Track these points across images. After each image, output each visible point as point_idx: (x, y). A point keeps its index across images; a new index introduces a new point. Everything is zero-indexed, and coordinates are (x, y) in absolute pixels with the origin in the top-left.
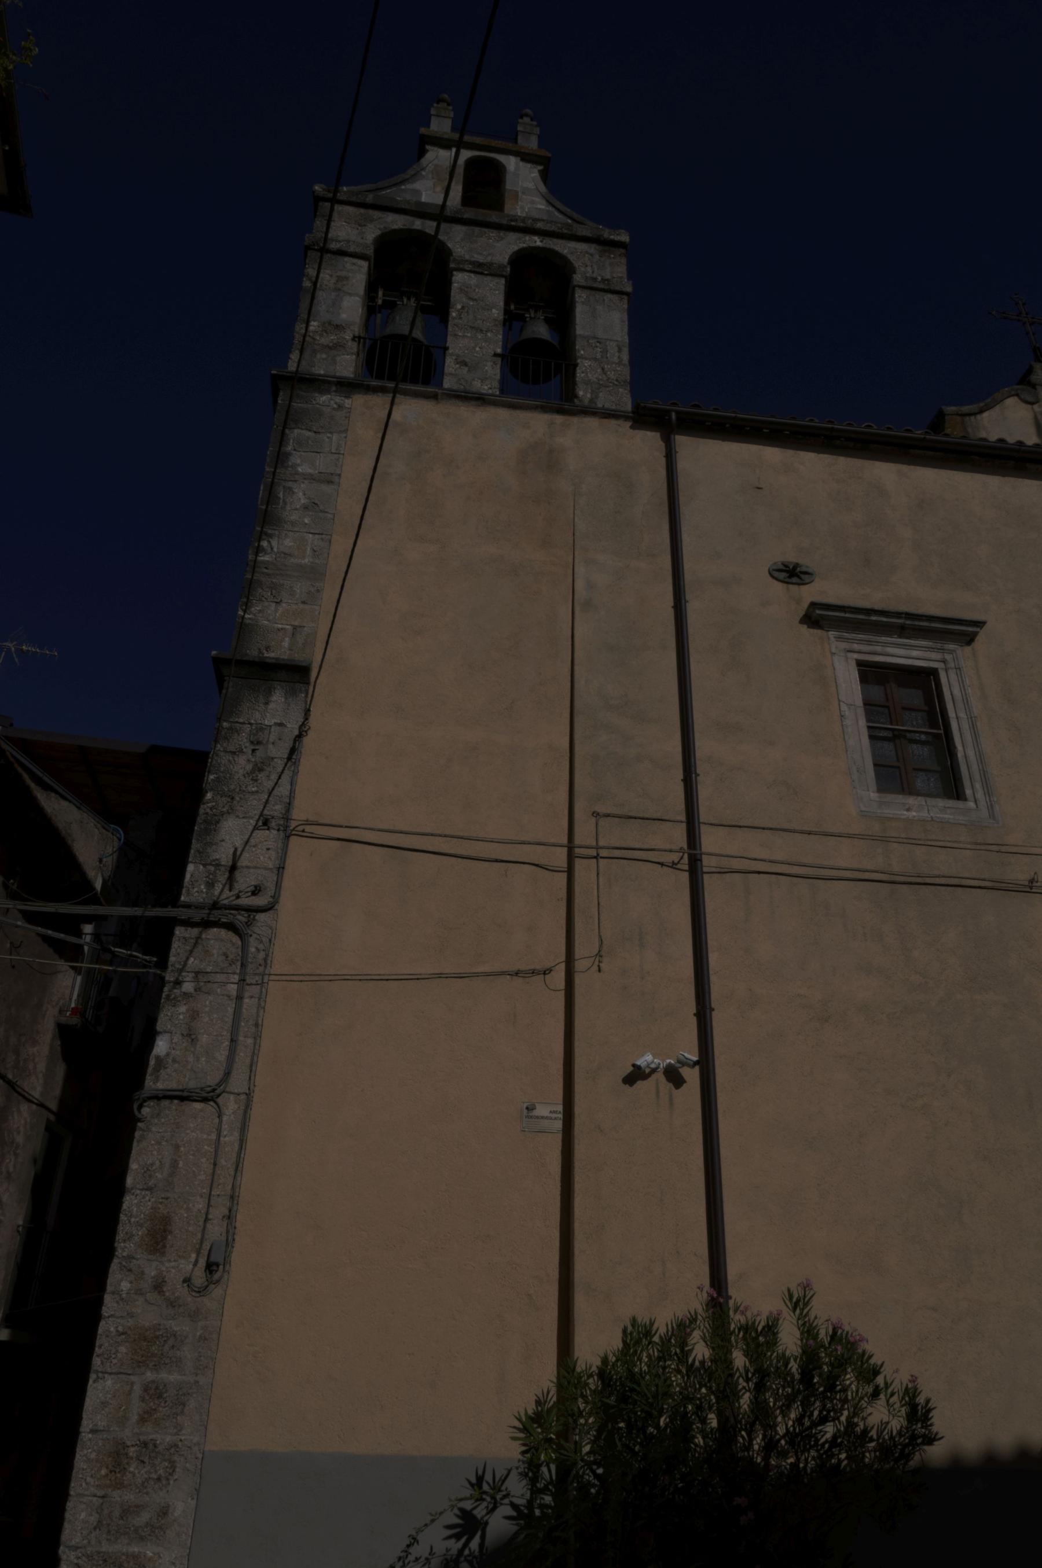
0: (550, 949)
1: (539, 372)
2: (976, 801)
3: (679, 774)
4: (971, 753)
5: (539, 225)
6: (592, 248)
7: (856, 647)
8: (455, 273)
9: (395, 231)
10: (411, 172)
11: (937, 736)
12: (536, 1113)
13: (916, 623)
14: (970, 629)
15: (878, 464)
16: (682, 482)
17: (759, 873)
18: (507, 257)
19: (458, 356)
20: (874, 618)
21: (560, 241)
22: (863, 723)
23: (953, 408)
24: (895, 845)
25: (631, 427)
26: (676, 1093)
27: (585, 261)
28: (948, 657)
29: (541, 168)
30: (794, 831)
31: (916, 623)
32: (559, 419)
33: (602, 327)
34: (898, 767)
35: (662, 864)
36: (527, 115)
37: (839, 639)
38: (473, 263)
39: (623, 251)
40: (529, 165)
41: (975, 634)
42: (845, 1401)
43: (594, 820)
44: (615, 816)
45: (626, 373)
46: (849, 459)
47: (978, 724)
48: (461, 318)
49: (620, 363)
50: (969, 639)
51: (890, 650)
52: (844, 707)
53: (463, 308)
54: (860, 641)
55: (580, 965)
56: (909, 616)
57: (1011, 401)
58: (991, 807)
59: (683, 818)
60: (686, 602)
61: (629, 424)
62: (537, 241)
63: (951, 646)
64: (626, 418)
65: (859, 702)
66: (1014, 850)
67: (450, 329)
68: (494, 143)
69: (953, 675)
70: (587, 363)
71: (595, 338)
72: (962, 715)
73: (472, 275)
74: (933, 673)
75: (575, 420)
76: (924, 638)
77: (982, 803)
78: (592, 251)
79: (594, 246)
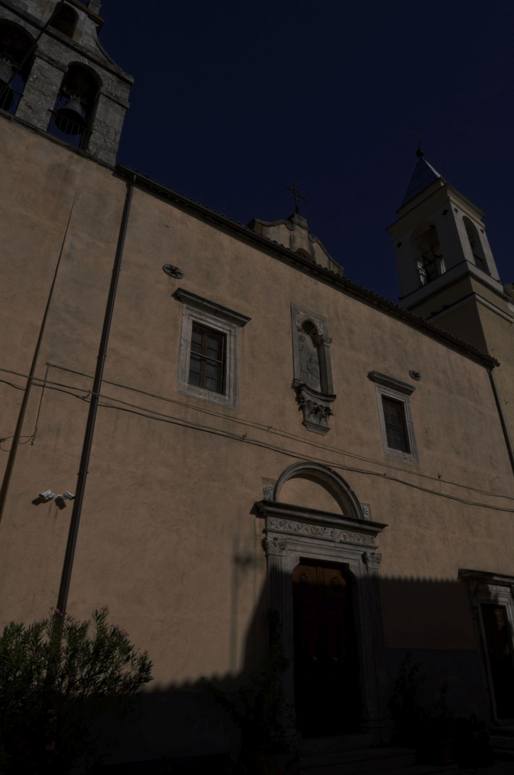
1: (71, 127)
2: (229, 397)
3: (97, 354)
4: (232, 375)
5: (89, 54)
6: (114, 78)
7: (194, 314)
8: (37, 58)
9: (7, 20)
11: (219, 364)
13: (223, 311)
14: (244, 320)
15: (223, 234)
16: (132, 211)
17: (125, 410)
18: (68, 63)
20: (205, 303)
21: (98, 67)
22: (189, 350)
24: (191, 409)
25: (112, 174)
26: (59, 511)
27: (108, 82)
28: (232, 330)
29: (98, 25)
30: (147, 394)
31: (223, 311)
32: (76, 156)
33: (109, 120)
34: (200, 374)
35: (78, 396)
37: (187, 308)
38: (49, 57)
39: (129, 86)
40: (91, 21)
41: (246, 322)
42: (112, 663)
43: (46, 367)
44: (58, 367)
45: (116, 147)
47: (238, 363)
48: (34, 83)
49: (114, 141)
50: (242, 324)
51: (208, 320)
52: (182, 341)
53: (37, 78)
55: (22, 440)
56: (220, 306)
57: (283, 226)
61: (112, 172)
62: (86, 62)
63: (235, 325)
64: (111, 169)
65: (190, 340)
67: (27, 86)
69: (232, 338)
70: (97, 134)
71: (104, 123)
72: (232, 357)
73: (47, 63)
74: (225, 335)
75: (85, 160)
76: (225, 318)
78: (114, 79)
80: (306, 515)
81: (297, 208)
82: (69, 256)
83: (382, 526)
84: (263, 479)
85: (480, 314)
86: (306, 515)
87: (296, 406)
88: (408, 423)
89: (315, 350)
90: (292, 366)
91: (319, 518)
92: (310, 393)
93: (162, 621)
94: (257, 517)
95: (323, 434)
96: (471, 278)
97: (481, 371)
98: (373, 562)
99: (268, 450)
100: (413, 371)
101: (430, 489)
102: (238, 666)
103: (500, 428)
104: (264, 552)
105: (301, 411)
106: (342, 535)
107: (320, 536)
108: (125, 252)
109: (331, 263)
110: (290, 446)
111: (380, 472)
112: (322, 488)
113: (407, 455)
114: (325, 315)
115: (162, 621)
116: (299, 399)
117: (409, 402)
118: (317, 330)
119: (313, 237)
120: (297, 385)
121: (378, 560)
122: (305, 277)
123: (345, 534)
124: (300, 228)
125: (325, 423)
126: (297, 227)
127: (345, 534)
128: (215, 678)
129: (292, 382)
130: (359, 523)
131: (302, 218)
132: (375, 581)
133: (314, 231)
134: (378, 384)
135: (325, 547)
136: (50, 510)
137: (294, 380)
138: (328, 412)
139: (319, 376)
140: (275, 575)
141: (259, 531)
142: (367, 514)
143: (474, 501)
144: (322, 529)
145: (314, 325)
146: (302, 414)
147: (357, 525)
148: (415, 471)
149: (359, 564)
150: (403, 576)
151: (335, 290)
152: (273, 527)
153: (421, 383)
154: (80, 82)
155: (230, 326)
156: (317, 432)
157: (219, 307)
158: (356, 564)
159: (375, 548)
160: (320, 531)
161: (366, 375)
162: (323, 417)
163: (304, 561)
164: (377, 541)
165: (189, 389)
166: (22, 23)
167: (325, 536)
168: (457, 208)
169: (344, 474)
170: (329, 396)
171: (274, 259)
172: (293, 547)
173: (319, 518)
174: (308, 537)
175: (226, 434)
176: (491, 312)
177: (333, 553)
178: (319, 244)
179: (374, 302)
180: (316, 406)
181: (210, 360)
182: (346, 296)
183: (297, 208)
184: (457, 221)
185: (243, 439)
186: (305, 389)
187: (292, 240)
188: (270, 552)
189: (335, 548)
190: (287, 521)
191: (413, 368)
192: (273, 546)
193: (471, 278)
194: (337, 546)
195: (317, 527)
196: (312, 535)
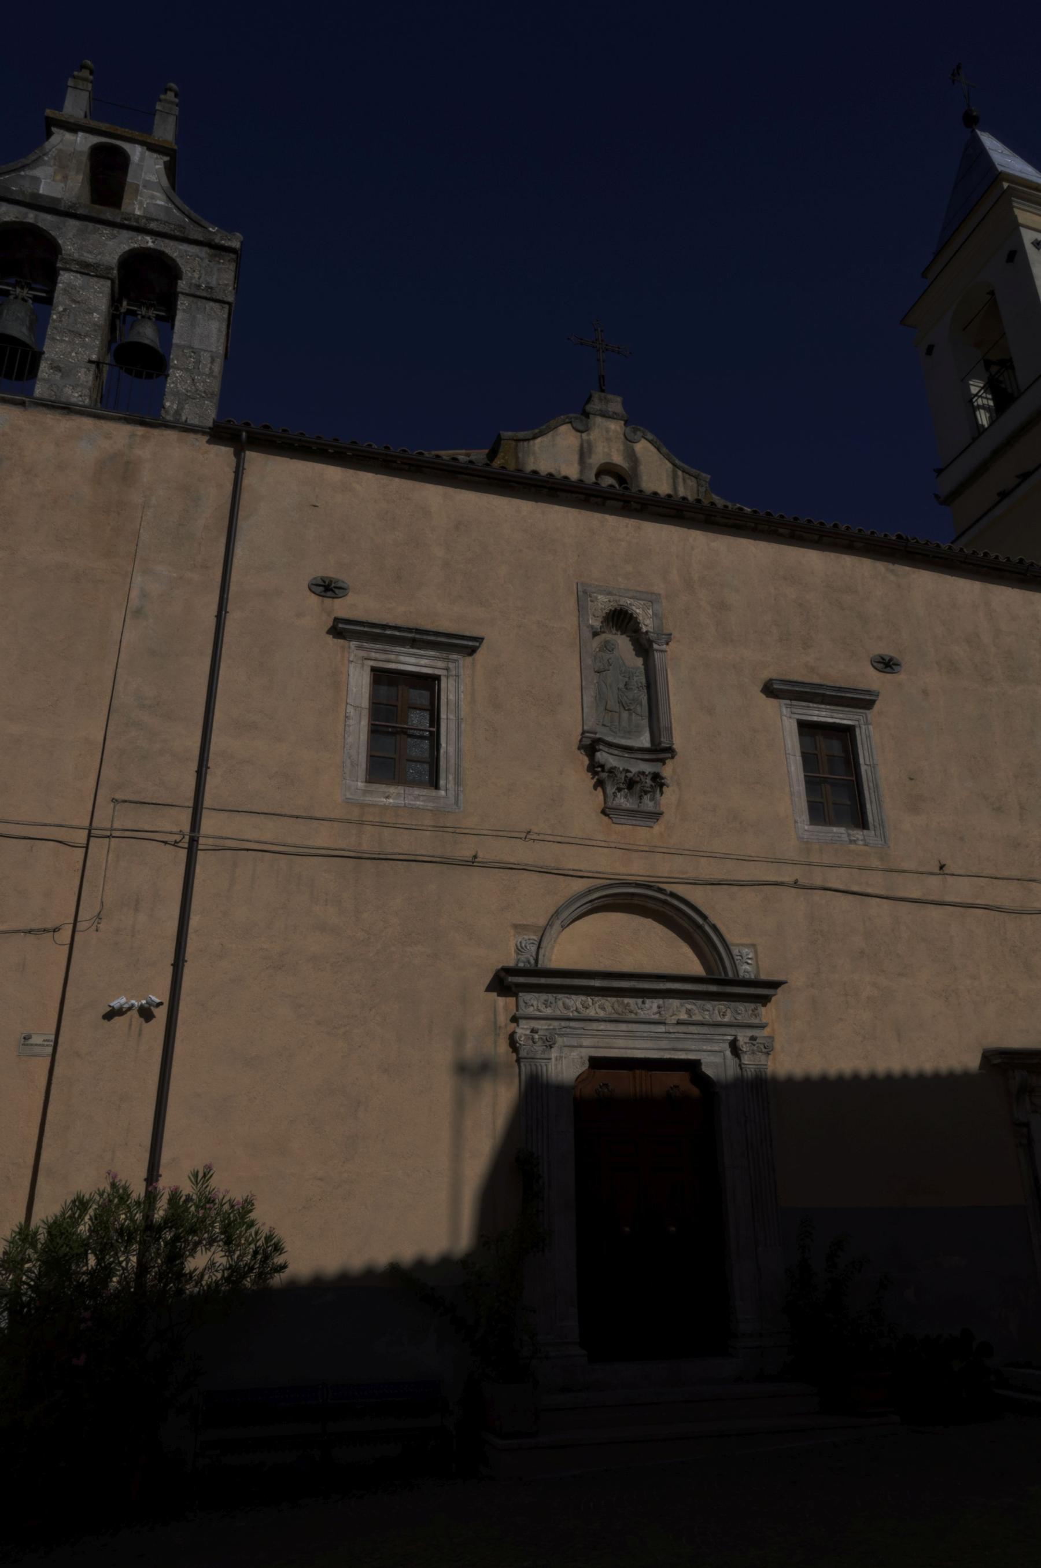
0: (62, 912)
1: (133, 379)
3: (194, 766)
4: (452, 750)
5: (153, 226)
6: (204, 252)
7: (373, 655)
8: (61, 272)
9: (7, 223)
10: (32, 157)
12: (30, 1042)
14: (470, 643)
16: (245, 498)
17: (248, 850)
18: (117, 257)
19: (53, 360)
20: (388, 632)
21: (172, 243)
22: (365, 723)
23: (509, 434)
24: (369, 827)
25: (208, 442)
26: (145, 1025)
27: (195, 267)
28: (451, 665)
29: (166, 159)
30: (285, 816)
32: (140, 430)
33: (199, 336)
35: (165, 843)
36: (171, 90)
37: (359, 648)
39: (234, 256)
40: (155, 155)
42: (239, 1245)
43: (112, 805)
44: (131, 802)
45: (215, 386)
46: (403, 481)
47: (463, 725)
48: (61, 321)
49: (211, 375)
50: (472, 651)
52: (350, 710)
53: (65, 310)
54: (377, 651)
55: (80, 926)
56: (418, 631)
57: (564, 429)
59: (191, 803)
60: (226, 612)
61: (206, 438)
62: (149, 242)
63: (455, 657)
64: (204, 433)
65: (365, 703)
67: (49, 332)
68: (120, 131)
69: (452, 681)
70: (178, 373)
71: (190, 347)
72: (452, 717)
73: (79, 276)
74: (437, 678)
75: (156, 432)
77: (451, 793)
78: (203, 255)
79: (206, 249)
80: (597, 983)
81: (601, 378)
82: (139, 612)
84: (516, 927)
86: (597, 983)
87: (589, 781)
88: (863, 768)
89: (640, 662)
90: (580, 707)
92: (616, 752)
93: (321, 1179)
95: (649, 824)
98: (753, 1053)
101: (915, 895)
102: (464, 1242)
104: (514, 1055)
105: (599, 789)
106: (684, 1010)
107: (633, 1016)
108: (235, 576)
109: (680, 473)
110: (573, 859)
111: (786, 879)
112: (655, 924)
113: (858, 834)
114: (659, 587)
115: (321, 1179)
116: (594, 767)
117: (867, 723)
119: (635, 431)
120: (587, 742)
121: (768, 1050)
122: (611, 520)
123: (689, 1006)
124: (604, 420)
125: (651, 804)
127: (689, 1006)
128: (420, 1264)
130: (726, 983)
131: (610, 397)
132: (760, 1088)
133: (637, 419)
134: (788, 702)
135: (645, 1034)
136: (130, 1025)
137: (583, 732)
140: (536, 1093)
141: (503, 1019)
145: (631, 615)
146: (601, 793)
147: (713, 988)
148: (875, 863)
151: (686, 530)
152: (530, 1011)
153: (902, 677)
154: (146, 283)
155: (447, 659)
156: (634, 822)
158: (717, 1059)
159: (762, 1027)
160: (633, 1006)
161: (756, 690)
162: (646, 793)
163: (596, 1063)
164: (767, 1013)
165: (365, 792)
166: (31, 217)
167: (642, 1015)
169: (696, 895)
170: (661, 751)
171: (540, 504)
172: (574, 1042)
174: (605, 1021)
175: (438, 860)
177: (664, 1044)
178: (651, 442)
179: (781, 531)
180: (629, 775)
181: (404, 731)
182: (710, 534)
183: (601, 378)
185: (473, 862)
186: (601, 747)
187: (584, 453)
188: (523, 1053)
190: (560, 996)
192: (530, 1042)
195: (626, 1000)
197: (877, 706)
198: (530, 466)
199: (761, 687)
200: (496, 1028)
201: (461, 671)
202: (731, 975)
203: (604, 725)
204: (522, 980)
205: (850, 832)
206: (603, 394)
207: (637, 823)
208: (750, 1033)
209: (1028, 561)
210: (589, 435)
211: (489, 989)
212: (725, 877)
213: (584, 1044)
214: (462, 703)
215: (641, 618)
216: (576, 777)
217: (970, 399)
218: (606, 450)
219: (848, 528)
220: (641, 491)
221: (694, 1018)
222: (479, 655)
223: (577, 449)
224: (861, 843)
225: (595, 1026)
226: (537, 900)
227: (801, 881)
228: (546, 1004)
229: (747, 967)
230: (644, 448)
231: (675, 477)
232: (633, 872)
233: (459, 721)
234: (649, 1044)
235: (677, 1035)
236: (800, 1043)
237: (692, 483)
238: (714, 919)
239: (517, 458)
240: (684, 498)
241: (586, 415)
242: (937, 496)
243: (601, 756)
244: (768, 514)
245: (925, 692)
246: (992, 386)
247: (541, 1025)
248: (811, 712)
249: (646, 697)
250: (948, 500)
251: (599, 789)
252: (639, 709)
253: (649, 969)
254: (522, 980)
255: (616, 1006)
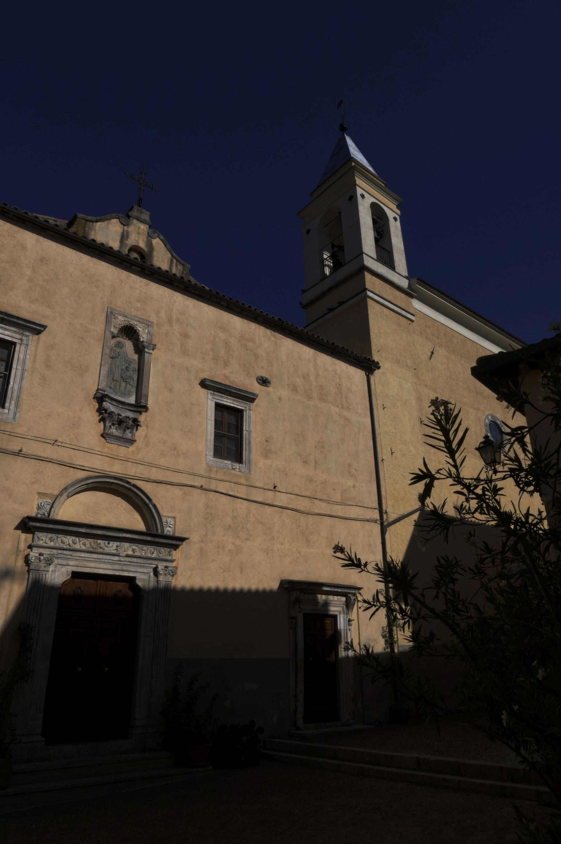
4: (16, 387)
11: (5, 375)
13: (10, 319)
14: (38, 328)
23: (83, 215)
28: (24, 338)
31: (10, 319)
41: (43, 331)
47: (26, 374)
50: (38, 332)
57: (114, 221)
58: (15, 414)
63: (28, 334)
66: (18, 435)
69: (23, 347)
72: (19, 368)
74: (14, 344)
77: (12, 412)
80: (83, 530)
81: (140, 199)
83: (183, 540)
84: (39, 494)
85: (369, 312)
86: (83, 530)
87: (96, 417)
88: (244, 432)
89: (136, 357)
91: (100, 532)
92: (115, 404)
94: (22, 532)
95: (127, 445)
96: (366, 273)
97: (357, 375)
98: (165, 575)
99: (51, 464)
100: (262, 377)
101: (260, 500)
103: (370, 435)
104: (27, 567)
105: (102, 423)
106: (131, 549)
107: (101, 550)
109: (175, 261)
111: (197, 484)
113: (237, 465)
114: (153, 319)
116: (101, 410)
117: (250, 410)
118: (139, 336)
119: (154, 232)
120: (99, 395)
121: (173, 573)
122: (133, 277)
123: (134, 547)
124: (138, 222)
125: (130, 435)
126: (135, 221)
127: (134, 547)
129: (95, 392)
131: (143, 210)
132: (167, 594)
133: (156, 227)
134: (212, 392)
137: (98, 390)
138: (136, 423)
139: (135, 385)
140: (37, 591)
141: (23, 546)
142: (170, 527)
143: (317, 511)
144: (105, 544)
145: (136, 330)
146: (103, 425)
147: (149, 539)
148: (243, 481)
149: (149, 577)
150: (206, 587)
153: (270, 389)
155: (23, 334)
156: (119, 443)
157: (5, 315)
159: (172, 561)
160: (102, 545)
162: (128, 428)
163: (75, 575)
164: (176, 554)
167: (107, 550)
168: (365, 193)
169: (147, 487)
170: (140, 407)
172: (64, 562)
173: (100, 532)
176: (385, 310)
177: (116, 567)
179: (222, 303)
183: (140, 199)
184: (361, 208)
185: (19, 453)
186: (107, 399)
187: (124, 237)
188: (32, 567)
189: (119, 562)
190: (60, 536)
191: (264, 374)
192: (38, 561)
193: (366, 273)
194: (122, 560)
195: (99, 541)
196: (92, 549)
197: (256, 401)
198: (92, 236)
199: (199, 382)
200: (18, 550)
201: (30, 343)
202: (159, 532)
203: (110, 388)
204: (38, 524)
205: (233, 464)
206: (140, 208)
207: (121, 444)
208: (165, 564)
209: (336, 344)
210: (128, 228)
211: (17, 528)
212: (165, 480)
213: (71, 564)
214: (27, 362)
215: (141, 333)
216: (90, 415)
217: (323, 260)
218: (136, 238)
219: (256, 309)
220: (152, 265)
221: (136, 554)
222: (42, 335)
223: (120, 234)
224: (237, 470)
225: (78, 554)
226: (54, 479)
227: (204, 486)
228: (51, 540)
229: (169, 529)
230: (157, 242)
231: (172, 262)
232: (114, 471)
233: (23, 371)
234: (108, 566)
235: (125, 563)
236: (191, 572)
237: (180, 267)
238: (155, 501)
239: (85, 230)
240: (175, 275)
241: (129, 217)
242: (301, 303)
243: (106, 405)
244: (217, 293)
245: (280, 399)
246: (333, 257)
247: (46, 552)
248: (223, 399)
249: (136, 377)
250: (306, 306)
251: (102, 423)
252: (132, 382)
253: (115, 525)
254: (38, 524)
255: (92, 544)
